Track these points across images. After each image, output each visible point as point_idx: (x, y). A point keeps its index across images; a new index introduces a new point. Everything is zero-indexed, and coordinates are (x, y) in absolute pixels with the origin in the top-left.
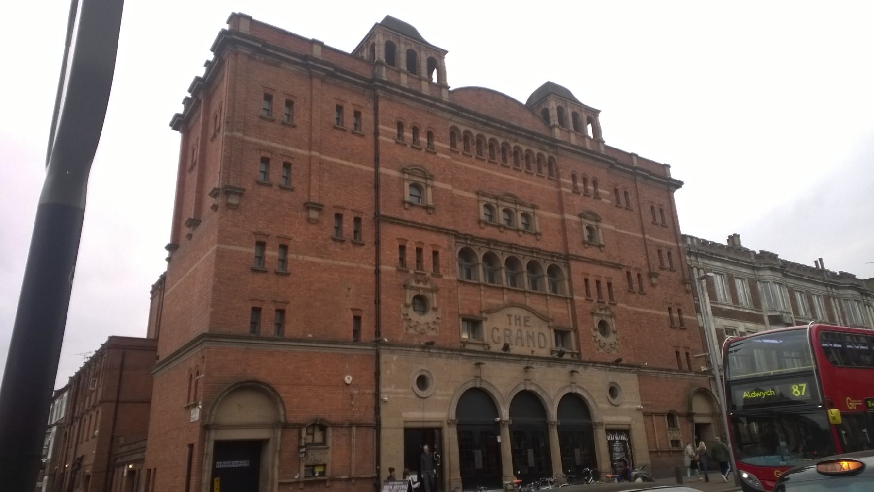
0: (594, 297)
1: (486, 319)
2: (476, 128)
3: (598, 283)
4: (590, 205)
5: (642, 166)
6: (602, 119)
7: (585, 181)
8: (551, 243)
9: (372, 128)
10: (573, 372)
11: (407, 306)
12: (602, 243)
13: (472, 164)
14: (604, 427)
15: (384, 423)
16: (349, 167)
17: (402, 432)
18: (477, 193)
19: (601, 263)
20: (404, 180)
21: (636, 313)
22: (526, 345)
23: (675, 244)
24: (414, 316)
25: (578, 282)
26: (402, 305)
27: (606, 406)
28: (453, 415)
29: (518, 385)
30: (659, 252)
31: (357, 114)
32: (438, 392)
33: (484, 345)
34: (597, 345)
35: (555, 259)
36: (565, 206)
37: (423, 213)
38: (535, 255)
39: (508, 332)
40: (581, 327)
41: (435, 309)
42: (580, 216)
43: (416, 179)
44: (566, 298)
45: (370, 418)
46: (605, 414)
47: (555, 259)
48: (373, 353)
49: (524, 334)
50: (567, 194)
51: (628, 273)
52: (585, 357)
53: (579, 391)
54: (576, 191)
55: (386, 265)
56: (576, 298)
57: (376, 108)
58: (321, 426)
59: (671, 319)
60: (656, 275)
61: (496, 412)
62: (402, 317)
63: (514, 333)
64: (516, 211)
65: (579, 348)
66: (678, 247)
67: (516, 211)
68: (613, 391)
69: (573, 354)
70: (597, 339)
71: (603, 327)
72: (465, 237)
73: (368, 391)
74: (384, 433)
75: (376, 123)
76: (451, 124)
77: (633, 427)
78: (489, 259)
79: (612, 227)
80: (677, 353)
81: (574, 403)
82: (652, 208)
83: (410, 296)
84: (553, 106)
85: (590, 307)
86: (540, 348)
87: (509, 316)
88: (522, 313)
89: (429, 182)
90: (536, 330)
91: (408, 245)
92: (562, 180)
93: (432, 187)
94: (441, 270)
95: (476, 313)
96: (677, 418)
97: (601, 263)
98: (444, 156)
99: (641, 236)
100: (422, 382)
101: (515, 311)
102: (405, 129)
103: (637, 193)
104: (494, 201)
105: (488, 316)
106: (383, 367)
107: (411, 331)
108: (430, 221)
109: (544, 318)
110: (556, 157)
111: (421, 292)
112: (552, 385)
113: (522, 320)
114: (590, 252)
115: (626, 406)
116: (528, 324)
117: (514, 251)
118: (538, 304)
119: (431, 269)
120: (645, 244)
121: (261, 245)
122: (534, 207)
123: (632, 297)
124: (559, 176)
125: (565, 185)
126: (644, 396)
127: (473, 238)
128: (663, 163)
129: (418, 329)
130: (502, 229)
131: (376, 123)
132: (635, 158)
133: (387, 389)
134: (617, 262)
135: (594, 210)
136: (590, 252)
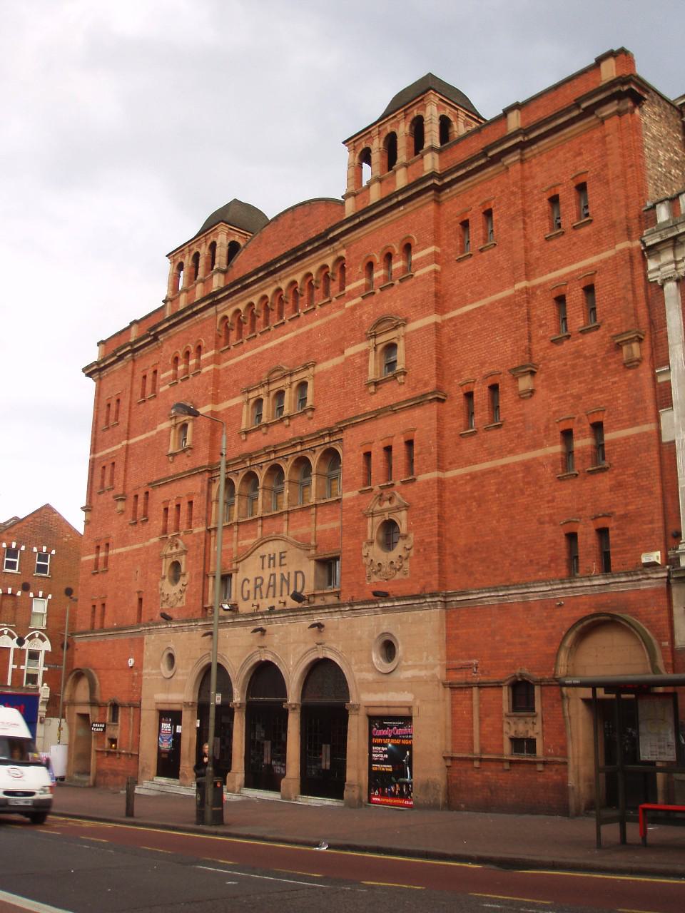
1: (237, 571)
13: (244, 351)
14: (362, 712)
21: (473, 476)
29: (252, 656)
46: (368, 691)
53: (330, 655)
58: (115, 707)
77: (415, 713)
80: (572, 537)
81: (323, 673)
84: (432, 112)
87: (263, 557)
90: (292, 569)
96: (537, 690)
105: (240, 565)
112: (292, 652)
115: (408, 674)
116: (284, 561)
121: (567, 435)
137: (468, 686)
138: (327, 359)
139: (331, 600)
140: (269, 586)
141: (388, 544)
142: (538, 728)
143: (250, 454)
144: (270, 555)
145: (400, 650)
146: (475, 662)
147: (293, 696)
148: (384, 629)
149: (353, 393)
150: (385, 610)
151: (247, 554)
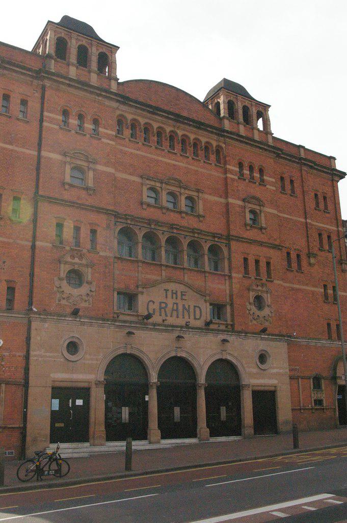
0: (253, 274)
1: (142, 293)
2: (143, 117)
3: (257, 262)
4: (256, 191)
5: (309, 158)
6: (271, 113)
7: (251, 168)
8: (215, 224)
9: (38, 115)
10: (224, 341)
11: (61, 279)
12: (264, 225)
15: (32, 382)
16: (12, 150)
17: (50, 390)
18: (141, 177)
19: (261, 244)
20: (65, 163)
21: (293, 289)
22: (180, 316)
23: (335, 229)
24: (67, 289)
25: (237, 260)
26: (56, 279)
27: (255, 370)
28: (101, 377)
30: (320, 235)
31: (24, 102)
32: (88, 356)
33: (138, 316)
34: (251, 317)
35: (216, 239)
36: (229, 191)
37: (83, 194)
38: (196, 235)
39: (163, 305)
40: (237, 301)
41: (89, 283)
42: (244, 200)
43: (79, 162)
44: (225, 275)
45: (20, 376)
46: (253, 378)
47: (216, 239)
48: (26, 321)
49: (180, 308)
50: (233, 180)
51: (288, 254)
52: (238, 327)
53: (229, 358)
54: (241, 176)
55: (41, 241)
56: (234, 275)
57: (43, 97)
59: (326, 296)
60: (315, 256)
61: (146, 374)
62: (55, 289)
63: (170, 306)
64: (181, 194)
65: (233, 320)
66: (338, 231)
67: (181, 194)
68: (263, 358)
69: (227, 326)
70: (251, 313)
71: (259, 302)
72: (126, 217)
73: (18, 354)
74: (31, 391)
75: (42, 112)
76: (118, 112)
77: (279, 388)
78: (150, 237)
79: (275, 212)
80: (329, 325)
81: (225, 368)
82: (316, 195)
83: (64, 269)
85: (246, 282)
86: (195, 319)
87: (166, 291)
88: (180, 288)
89: (91, 165)
90: (192, 304)
91: (65, 224)
92: (228, 167)
93: (94, 170)
94: (98, 248)
95: (132, 287)
96: (323, 381)
97: (261, 244)
98: (108, 141)
99: (303, 220)
100: (73, 347)
101: (172, 286)
102: (70, 116)
103: (302, 181)
104: (158, 185)
106: (33, 333)
107: (64, 302)
108: (90, 201)
109: (202, 293)
110: (224, 146)
111: (76, 267)
112: (203, 352)
113: (179, 294)
114: (252, 234)
115: (275, 371)
116: (184, 297)
117: (175, 231)
118: (198, 281)
119: (89, 246)
120: (307, 227)
122: (198, 191)
123: (290, 275)
124: (225, 164)
125: (231, 172)
126: (291, 361)
127: (133, 219)
128: (329, 155)
129: (70, 301)
130: (164, 211)
131: (42, 112)
132: (302, 151)
133: (37, 353)
134: (277, 243)
135: (258, 195)
136: (252, 234)
137: (297, 378)
138: (210, 194)
139: (222, 327)
140: (173, 310)
141: (260, 308)
142: (324, 395)
143: (159, 222)
144: (172, 291)
145: (270, 361)
146: (298, 367)
147: (202, 379)
148: (261, 348)
149: (235, 223)
150: (262, 339)
151: (154, 284)
